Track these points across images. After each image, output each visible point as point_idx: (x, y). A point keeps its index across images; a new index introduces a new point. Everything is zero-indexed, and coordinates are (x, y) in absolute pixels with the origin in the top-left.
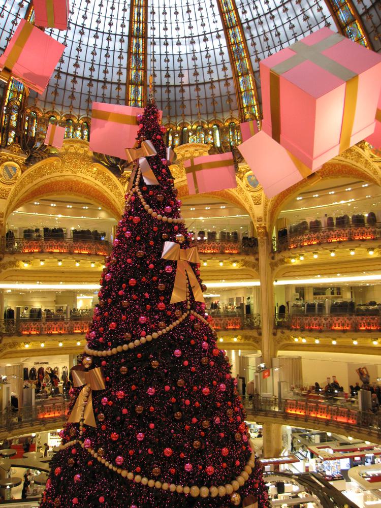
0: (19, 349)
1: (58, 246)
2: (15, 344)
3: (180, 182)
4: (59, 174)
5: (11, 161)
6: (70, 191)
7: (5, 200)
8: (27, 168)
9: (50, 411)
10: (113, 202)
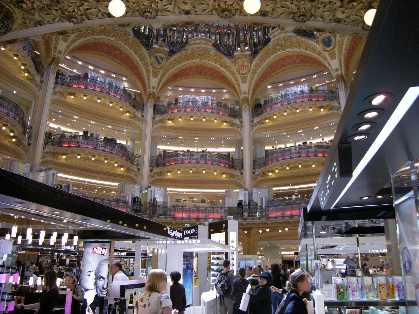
0: (164, 177)
2: (161, 173)
10: (229, 79)
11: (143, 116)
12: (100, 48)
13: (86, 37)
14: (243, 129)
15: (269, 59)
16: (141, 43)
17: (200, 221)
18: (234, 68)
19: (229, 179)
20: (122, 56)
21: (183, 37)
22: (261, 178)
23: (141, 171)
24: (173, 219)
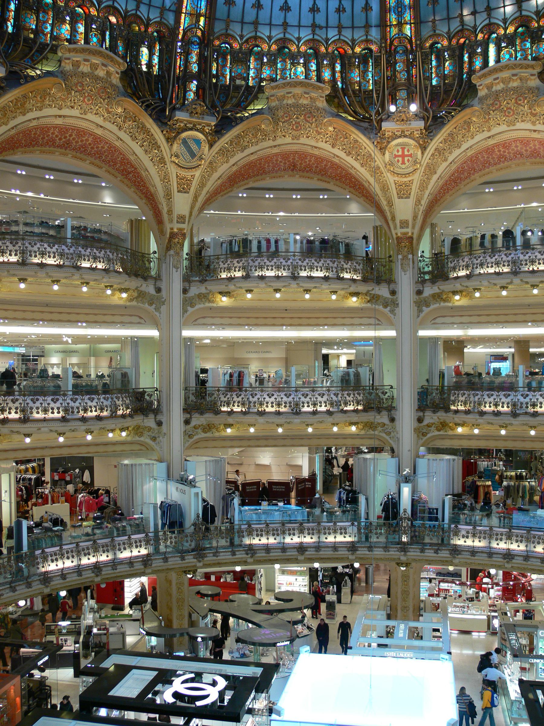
0: (217, 434)
1: (272, 266)
3: (485, 139)
4: (271, 143)
5: (191, 129)
6: (293, 170)
7: (186, 195)
8: (219, 139)
9: (262, 535)
10: (366, 185)
11: (159, 290)
12: (43, 138)
13: (6, 125)
14: (397, 311)
15: (471, 142)
16: (146, 110)
17: (307, 553)
18: (380, 160)
19: (363, 432)
20: (97, 147)
21: (249, 74)
22: (437, 433)
23: (164, 427)
24: (247, 554)
